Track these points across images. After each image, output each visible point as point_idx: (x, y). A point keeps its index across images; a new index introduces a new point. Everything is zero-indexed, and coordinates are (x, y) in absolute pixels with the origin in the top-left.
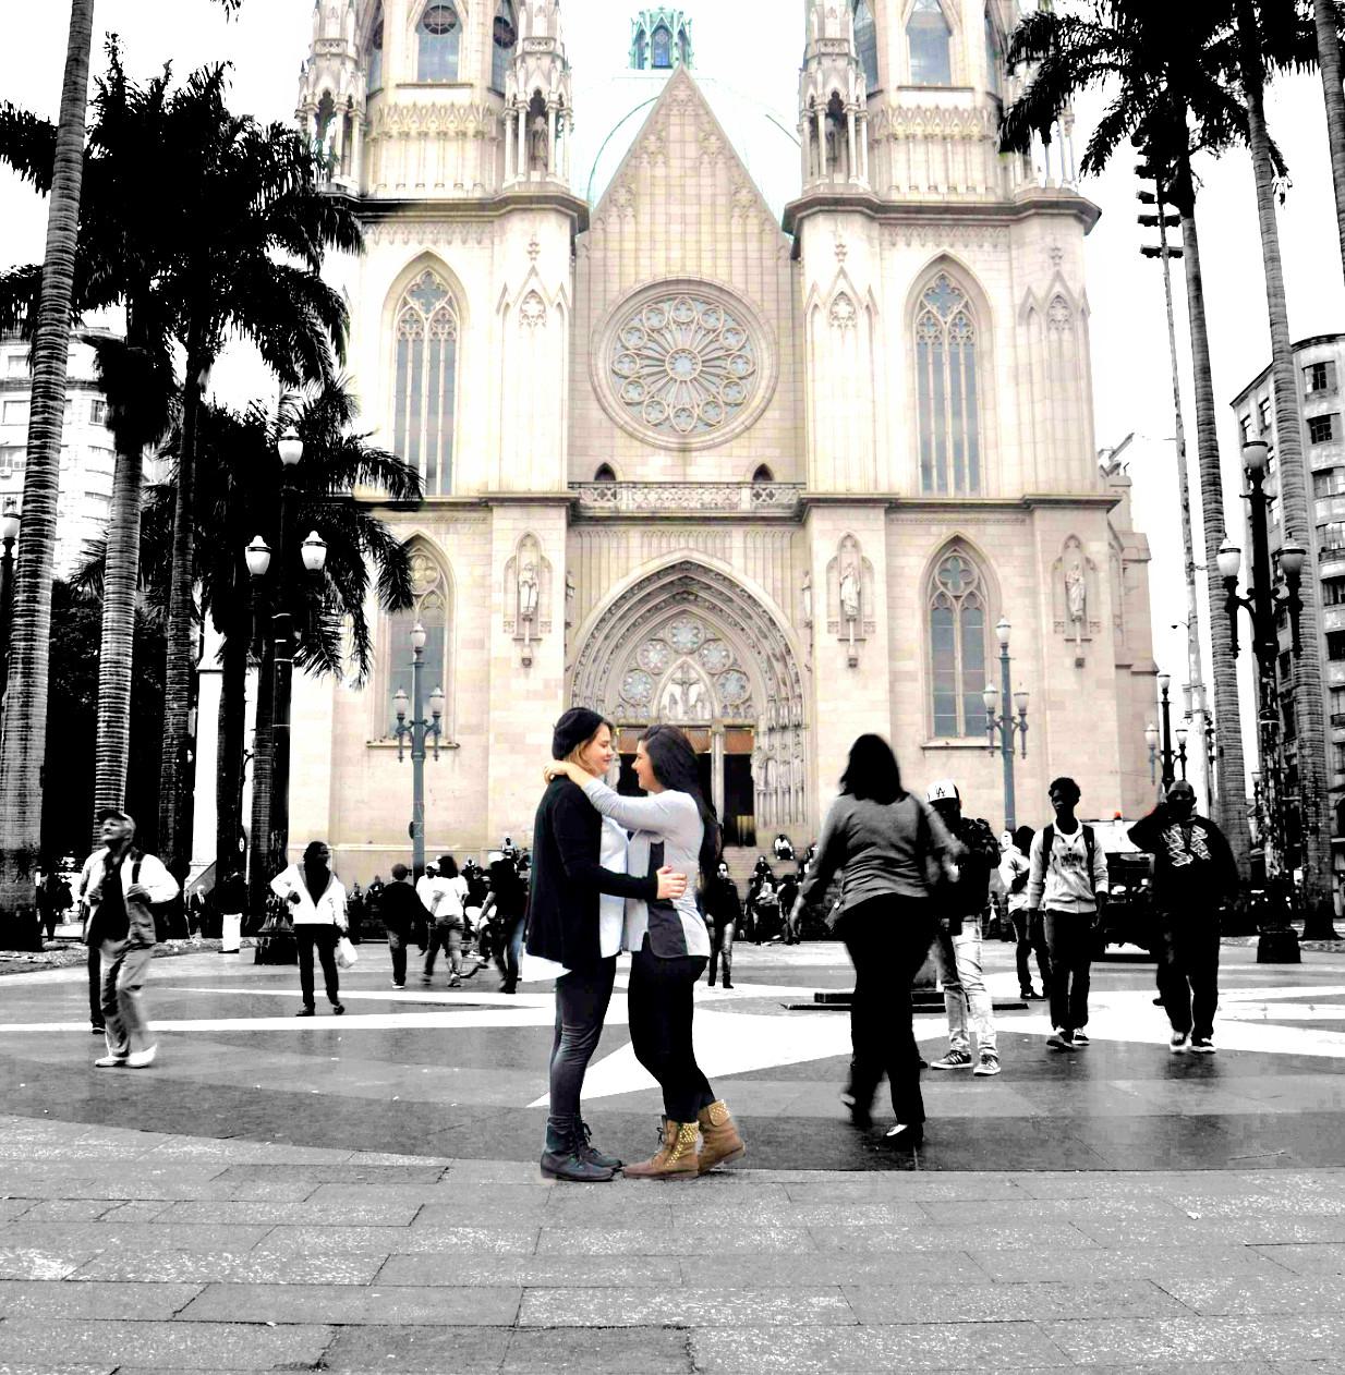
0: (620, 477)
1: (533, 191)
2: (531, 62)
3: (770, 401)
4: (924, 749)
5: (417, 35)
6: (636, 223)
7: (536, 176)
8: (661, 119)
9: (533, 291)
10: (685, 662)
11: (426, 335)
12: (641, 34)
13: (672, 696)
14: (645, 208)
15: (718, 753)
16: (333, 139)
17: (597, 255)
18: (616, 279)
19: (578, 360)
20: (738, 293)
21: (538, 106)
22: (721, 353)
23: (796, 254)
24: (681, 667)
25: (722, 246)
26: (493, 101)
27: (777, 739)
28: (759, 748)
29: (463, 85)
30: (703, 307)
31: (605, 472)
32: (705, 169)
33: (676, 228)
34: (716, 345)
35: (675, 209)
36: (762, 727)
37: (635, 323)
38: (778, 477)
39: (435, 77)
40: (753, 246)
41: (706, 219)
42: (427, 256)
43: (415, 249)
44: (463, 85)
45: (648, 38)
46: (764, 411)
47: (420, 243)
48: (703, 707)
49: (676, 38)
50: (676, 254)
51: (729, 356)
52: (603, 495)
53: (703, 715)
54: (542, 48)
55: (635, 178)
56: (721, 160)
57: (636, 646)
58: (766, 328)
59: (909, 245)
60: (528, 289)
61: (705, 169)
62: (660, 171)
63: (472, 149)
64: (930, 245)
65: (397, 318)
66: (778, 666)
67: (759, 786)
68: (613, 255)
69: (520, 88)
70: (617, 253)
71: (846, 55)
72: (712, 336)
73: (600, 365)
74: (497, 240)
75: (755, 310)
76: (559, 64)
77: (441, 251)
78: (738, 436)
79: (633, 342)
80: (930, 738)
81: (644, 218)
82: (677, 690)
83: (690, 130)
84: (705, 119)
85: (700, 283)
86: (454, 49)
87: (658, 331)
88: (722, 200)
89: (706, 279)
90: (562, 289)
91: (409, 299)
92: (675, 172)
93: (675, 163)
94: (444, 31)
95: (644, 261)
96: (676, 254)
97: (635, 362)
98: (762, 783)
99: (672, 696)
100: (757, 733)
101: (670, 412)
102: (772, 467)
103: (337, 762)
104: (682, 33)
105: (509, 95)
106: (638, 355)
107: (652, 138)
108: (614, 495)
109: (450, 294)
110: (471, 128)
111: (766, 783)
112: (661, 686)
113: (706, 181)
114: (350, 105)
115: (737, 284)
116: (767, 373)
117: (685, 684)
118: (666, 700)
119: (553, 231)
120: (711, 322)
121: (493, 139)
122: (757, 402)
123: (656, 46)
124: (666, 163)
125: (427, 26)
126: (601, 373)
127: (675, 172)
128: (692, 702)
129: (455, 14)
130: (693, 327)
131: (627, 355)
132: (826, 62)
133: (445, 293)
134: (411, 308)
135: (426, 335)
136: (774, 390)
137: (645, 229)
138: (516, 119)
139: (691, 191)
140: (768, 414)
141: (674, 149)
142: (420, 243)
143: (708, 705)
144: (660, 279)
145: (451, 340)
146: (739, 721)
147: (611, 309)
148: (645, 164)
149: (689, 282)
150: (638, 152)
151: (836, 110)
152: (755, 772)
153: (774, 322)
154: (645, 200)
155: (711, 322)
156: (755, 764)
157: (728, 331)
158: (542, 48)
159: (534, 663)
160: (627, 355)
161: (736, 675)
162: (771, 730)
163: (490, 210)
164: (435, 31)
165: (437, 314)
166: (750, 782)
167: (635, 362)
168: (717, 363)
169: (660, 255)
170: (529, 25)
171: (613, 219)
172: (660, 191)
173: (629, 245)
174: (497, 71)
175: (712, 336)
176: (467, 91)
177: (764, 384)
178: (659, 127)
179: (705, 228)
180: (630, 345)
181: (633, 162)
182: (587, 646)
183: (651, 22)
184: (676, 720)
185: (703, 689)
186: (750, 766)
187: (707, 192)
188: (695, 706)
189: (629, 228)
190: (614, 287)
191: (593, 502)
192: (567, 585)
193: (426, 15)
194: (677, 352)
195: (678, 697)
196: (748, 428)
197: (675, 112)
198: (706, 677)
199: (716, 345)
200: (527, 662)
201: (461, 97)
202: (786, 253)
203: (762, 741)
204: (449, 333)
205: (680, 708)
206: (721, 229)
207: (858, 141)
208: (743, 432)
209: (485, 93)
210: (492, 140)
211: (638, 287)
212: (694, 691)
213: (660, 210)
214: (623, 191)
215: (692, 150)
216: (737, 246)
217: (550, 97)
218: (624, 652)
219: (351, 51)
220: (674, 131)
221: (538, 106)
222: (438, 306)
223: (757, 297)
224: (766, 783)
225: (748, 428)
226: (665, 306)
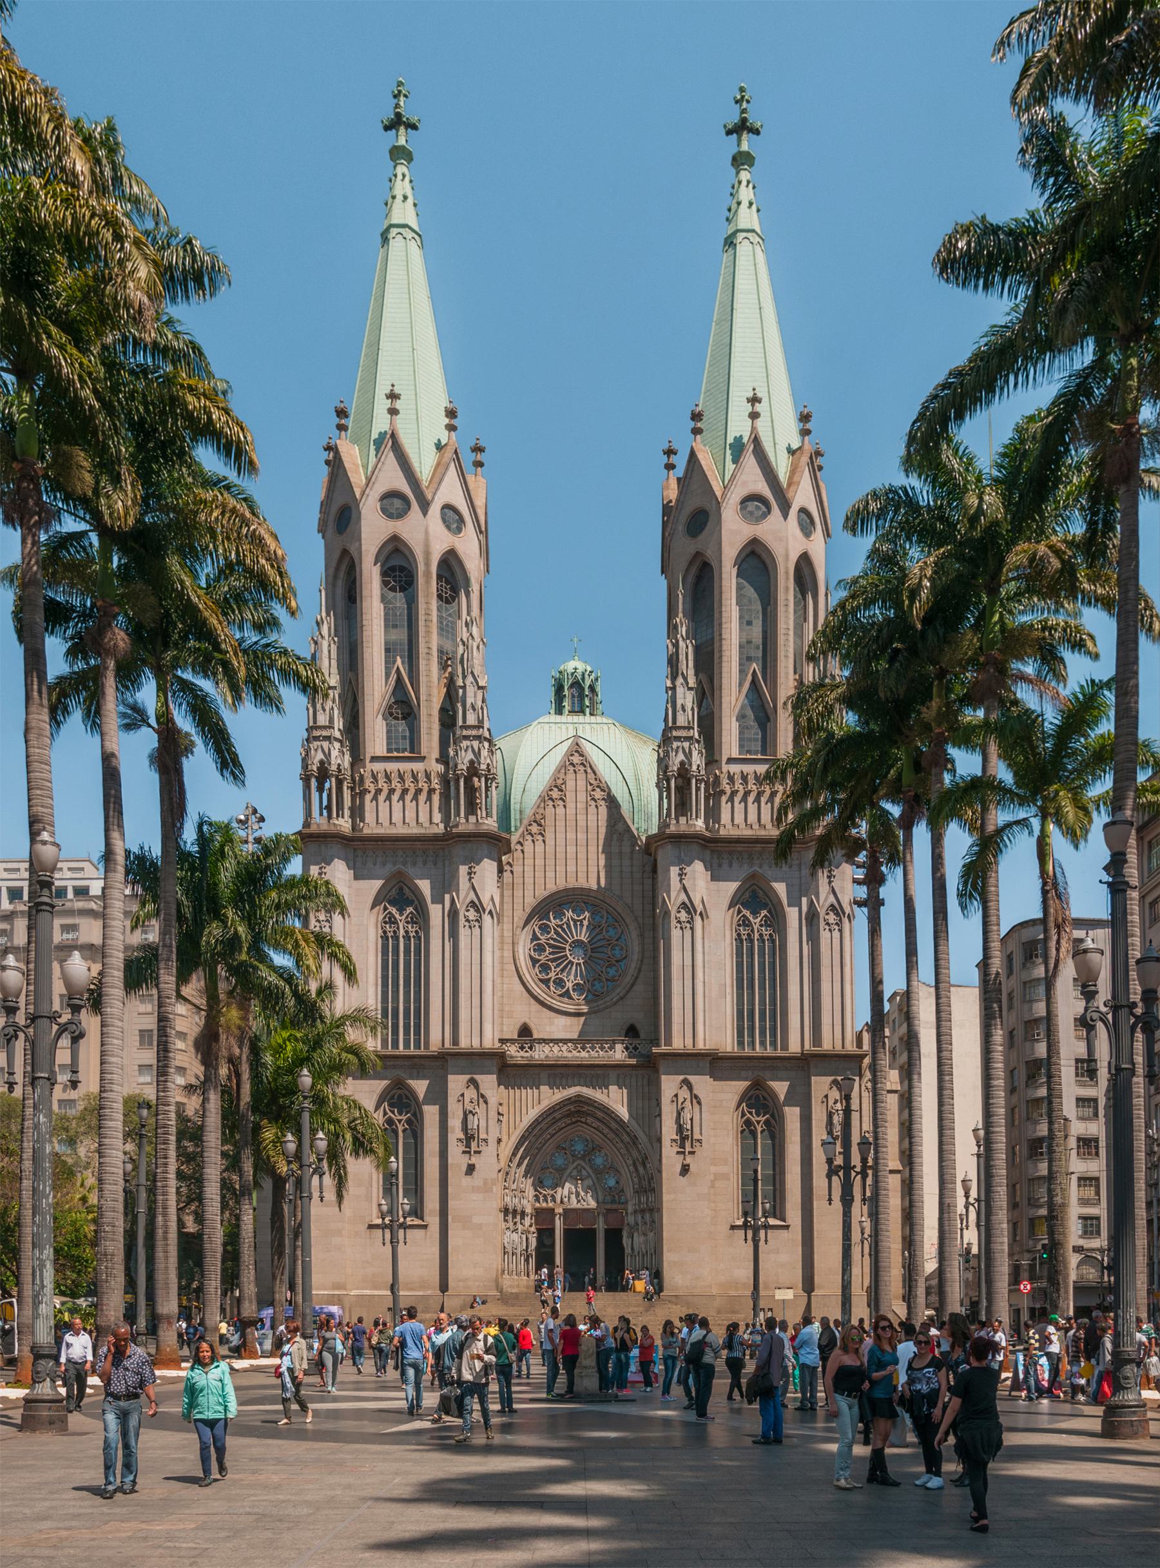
0: (535, 1036)
3: (637, 978)
14: (549, 836)
15: (601, 1226)
17: (517, 869)
19: (506, 947)
22: (603, 943)
23: (654, 870)
31: (525, 1031)
32: (592, 809)
34: (599, 937)
36: (630, 1209)
38: (642, 1035)
46: (633, 985)
47: (395, 864)
50: (571, 868)
52: (522, 1048)
59: (730, 866)
62: (560, 810)
64: (745, 867)
66: (641, 1169)
67: (628, 1251)
71: (692, 738)
72: (597, 930)
73: (521, 951)
74: (447, 863)
78: (615, 1004)
90: (492, 899)
96: (571, 868)
101: (569, 985)
102: (638, 1027)
108: (531, 1048)
116: (636, 957)
122: (628, 979)
126: (522, 958)
136: (640, 970)
139: (582, 823)
140: (635, 988)
142: (395, 864)
151: (684, 773)
152: (626, 1241)
153: (641, 920)
156: (625, 1234)
162: (635, 1212)
166: (623, 1249)
171: (528, 846)
172: (560, 824)
175: (597, 930)
177: (633, 965)
186: (621, 1237)
190: (529, 893)
191: (512, 1050)
192: (499, 1114)
196: (622, 998)
199: (599, 937)
200: (471, 1169)
202: (648, 868)
203: (631, 1219)
207: (698, 796)
208: (618, 1001)
215: (582, 797)
225: (622, 998)
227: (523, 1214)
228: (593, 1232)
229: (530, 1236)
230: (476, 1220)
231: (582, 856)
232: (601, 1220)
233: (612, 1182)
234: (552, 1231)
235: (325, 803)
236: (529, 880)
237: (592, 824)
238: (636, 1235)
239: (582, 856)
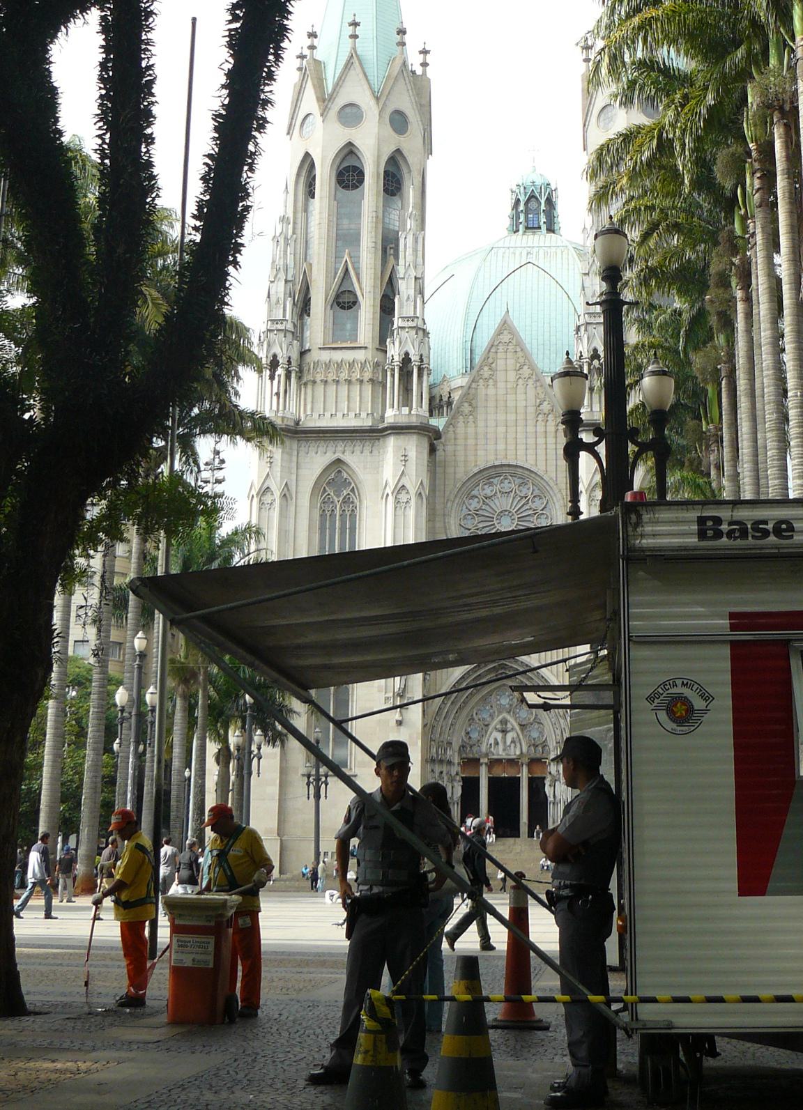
1: (403, 421)
2: (404, 334)
5: (330, 313)
6: (476, 427)
7: (405, 410)
8: (491, 355)
9: (403, 486)
10: (504, 718)
11: (338, 512)
12: (518, 202)
13: (496, 739)
14: (481, 417)
15: (524, 775)
16: (279, 376)
17: (450, 448)
18: (461, 464)
20: (541, 473)
21: (406, 360)
22: (530, 512)
24: (501, 722)
25: (531, 441)
26: (378, 357)
28: (550, 773)
29: (360, 348)
30: (518, 481)
33: (501, 430)
34: (527, 507)
35: (501, 417)
37: (475, 492)
39: (340, 336)
40: (551, 440)
41: (521, 423)
42: (339, 461)
43: (330, 457)
44: (360, 348)
45: (522, 207)
48: (515, 747)
49: (543, 207)
51: (535, 514)
53: (514, 752)
54: (411, 324)
55: (475, 396)
56: (531, 382)
57: (473, 708)
58: (559, 496)
60: (400, 485)
61: (521, 388)
62: (491, 391)
63: (368, 389)
65: (320, 501)
67: (551, 799)
68: (460, 448)
69: (394, 351)
70: (462, 448)
72: (524, 501)
73: (452, 522)
75: (552, 484)
76: (421, 333)
77: (347, 458)
79: (474, 504)
81: (481, 424)
82: (499, 736)
83: (511, 362)
84: (520, 354)
85: (516, 466)
86: (356, 318)
87: (489, 498)
88: (531, 410)
89: (520, 464)
91: (327, 488)
92: (501, 391)
93: (501, 385)
94: (350, 308)
95: (481, 453)
96: (501, 447)
97: (474, 518)
98: (552, 796)
99: (496, 739)
104: (550, 202)
105: (389, 355)
106: (477, 514)
107: (486, 368)
109: (353, 485)
110: (367, 375)
111: (554, 796)
112: (489, 733)
113: (521, 397)
114: (289, 362)
115: (540, 469)
117: (504, 732)
118: (492, 741)
119: (414, 447)
120: (524, 491)
121: (381, 383)
123: (527, 212)
124: (495, 385)
125: (338, 304)
127: (501, 391)
128: (508, 743)
129: (355, 295)
130: (512, 494)
131: (469, 514)
132: (590, 328)
133: (350, 483)
134: (329, 494)
135: (338, 512)
137: (481, 430)
138: (393, 370)
139: (511, 404)
141: (500, 376)
143: (518, 745)
144: (490, 464)
145: (353, 516)
146: (538, 756)
147: (459, 485)
148: (481, 386)
149: (509, 466)
150: (477, 379)
152: (548, 790)
154: (481, 410)
155: (524, 491)
156: (547, 783)
157: (535, 497)
158: (411, 324)
159: (404, 722)
160: (469, 514)
161: (536, 726)
163: (374, 434)
164: (343, 308)
165: (344, 499)
167: (474, 518)
168: (527, 519)
169: (491, 447)
170: (401, 307)
171: (461, 425)
172: (491, 404)
173: (471, 442)
174: (382, 341)
175: (524, 501)
176: (363, 351)
178: (490, 360)
179: (519, 429)
180: (471, 508)
181: (474, 385)
182: (440, 708)
183: (526, 193)
184: (498, 755)
185: (515, 735)
187: (521, 404)
188: (510, 746)
189: (471, 430)
193: (337, 296)
194: (501, 512)
195: (499, 740)
197: (501, 350)
198: (517, 728)
199: (527, 507)
201: (360, 356)
204: (353, 510)
205: (501, 747)
206: (530, 429)
209: (375, 351)
210: (379, 384)
211: (476, 470)
212: (510, 736)
213: (491, 417)
214: (466, 404)
215: (512, 376)
216: (541, 441)
217: (414, 358)
218: (465, 712)
219: (290, 326)
220: (501, 363)
221: (406, 360)
222: (345, 493)
223: (553, 475)
224: (554, 796)
226: (495, 481)
227: (450, 763)
228: (516, 782)
229: (455, 784)
231: (511, 436)
232: (525, 769)
233: (535, 735)
234: (477, 780)
235: (275, 390)
236: (461, 458)
237: (521, 404)
239: (511, 436)
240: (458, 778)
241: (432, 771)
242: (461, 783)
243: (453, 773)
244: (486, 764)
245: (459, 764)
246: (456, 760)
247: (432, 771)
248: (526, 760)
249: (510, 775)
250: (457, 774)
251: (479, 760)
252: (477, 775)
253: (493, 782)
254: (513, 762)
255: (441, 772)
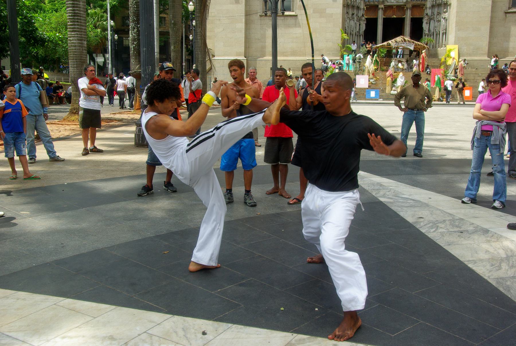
4: (506, 13)
15: (408, 16)
27: (436, 10)
28: (427, 14)
80: (509, 8)
98: (427, 30)
100: (426, 8)
103: (248, 23)
111: (429, 30)
152: (425, 26)
156: (425, 21)
162: (433, 6)
186: (422, 22)
203: (429, 12)
224: (429, 30)
227: (358, 8)
230: (328, 11)
234: (375, 20)
238: (432, 22)
240: (363, 18)
241: (347, 13)
242: (365, 22)
243: (360, 14)
244: (382, 8)
245: (364, 9)
246: (362, 6)
247: (347, 13)
248: (409, 6)
249: (398, 17)
250: (363, 15)
251: (378, 6)
252: (375, 17)
253: (385, 20)
254: (401, 8)
255: (353, 14)
